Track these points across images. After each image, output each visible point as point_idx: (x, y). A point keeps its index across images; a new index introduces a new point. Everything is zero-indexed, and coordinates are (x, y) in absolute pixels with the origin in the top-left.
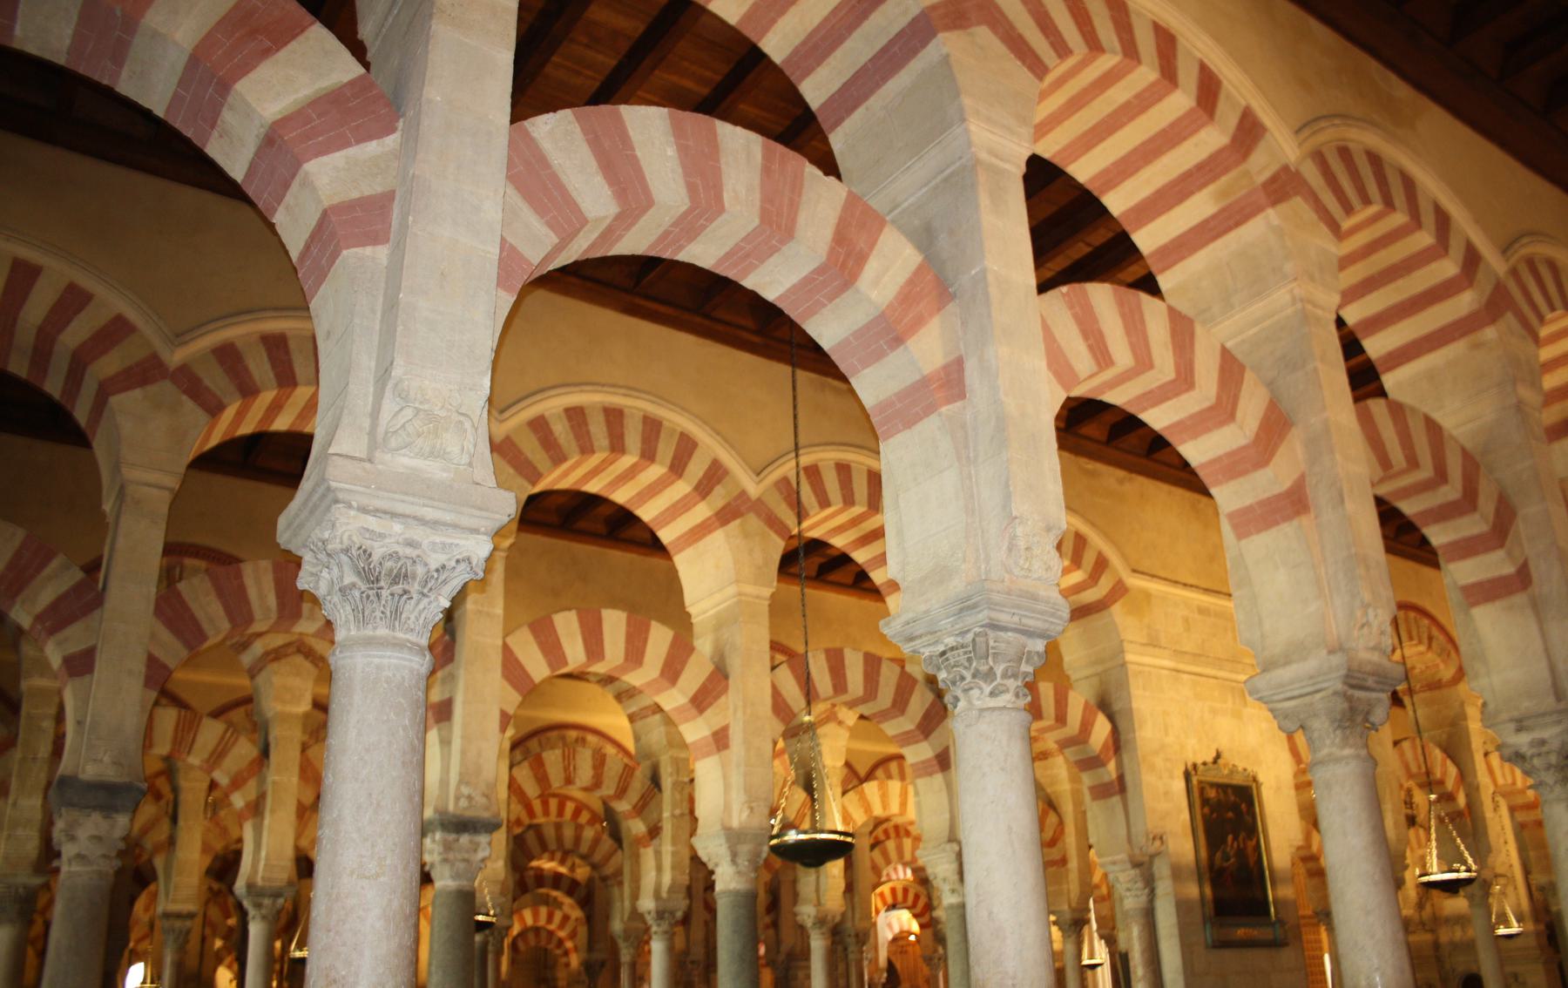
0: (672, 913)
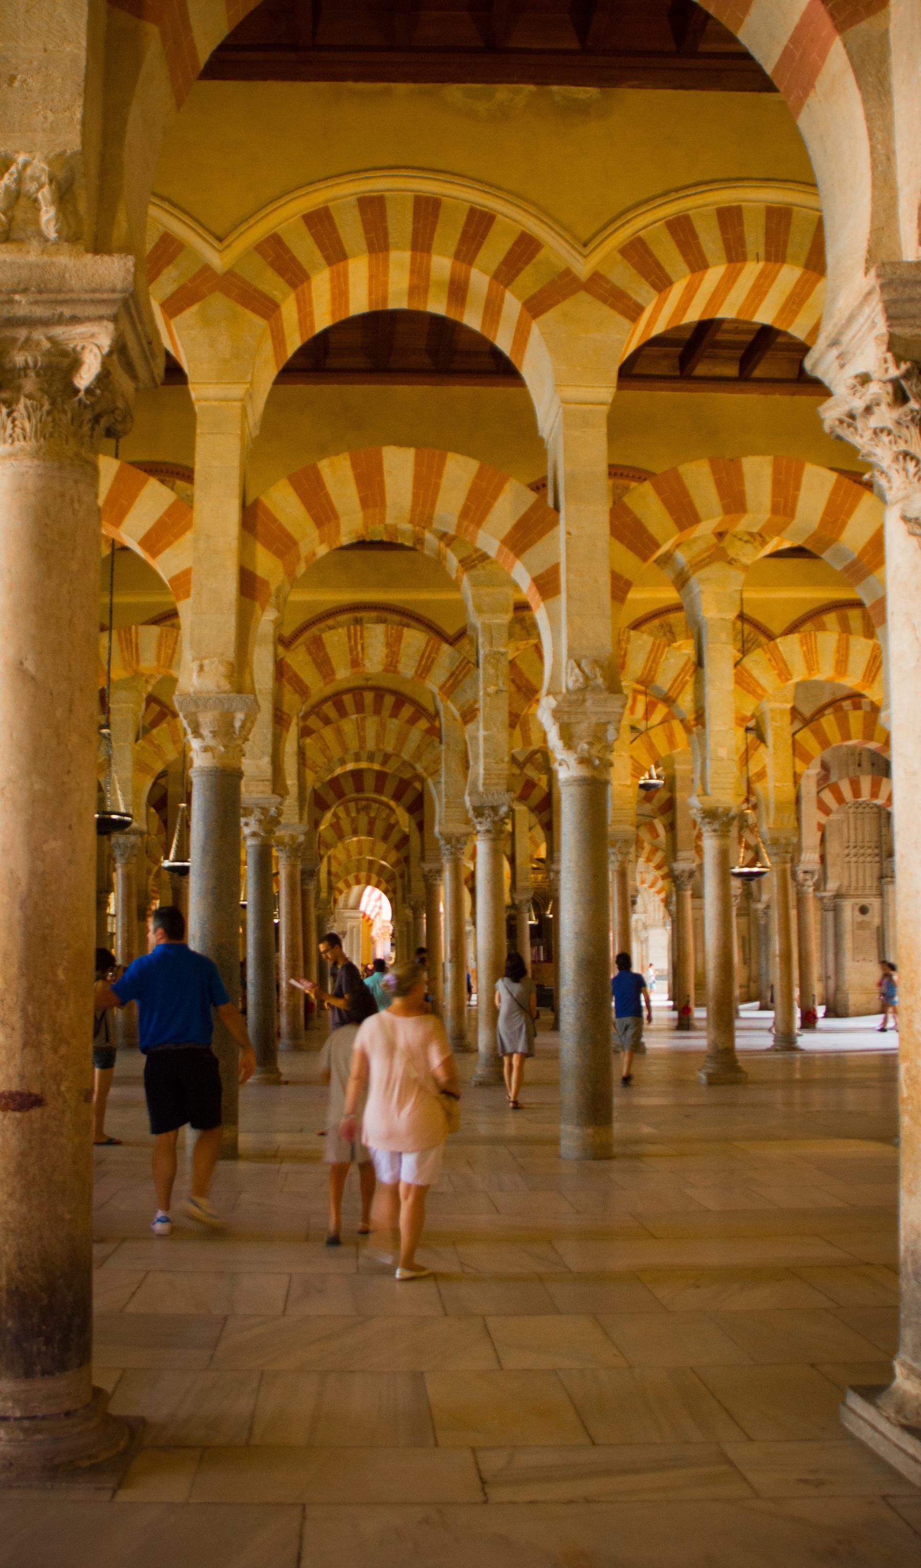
0: (495, 809)
